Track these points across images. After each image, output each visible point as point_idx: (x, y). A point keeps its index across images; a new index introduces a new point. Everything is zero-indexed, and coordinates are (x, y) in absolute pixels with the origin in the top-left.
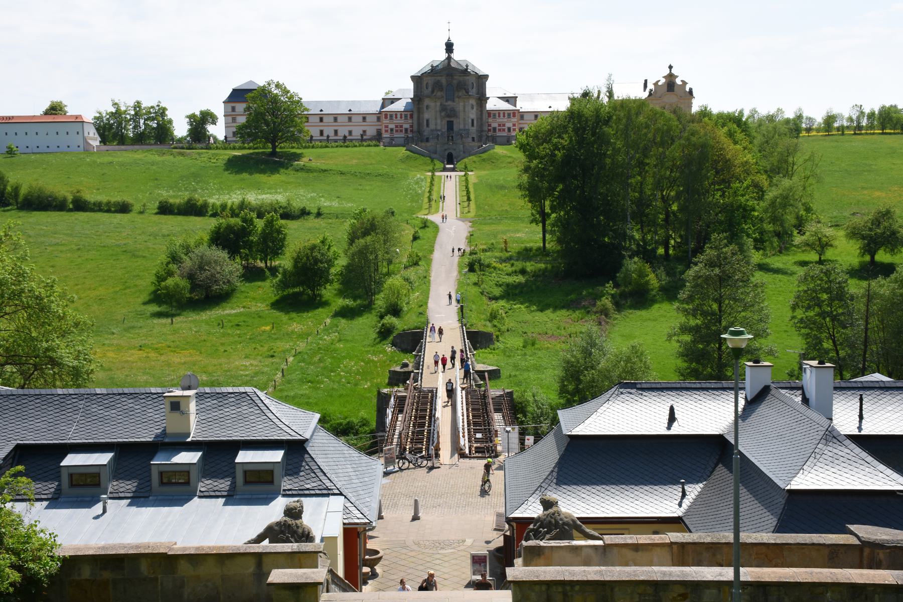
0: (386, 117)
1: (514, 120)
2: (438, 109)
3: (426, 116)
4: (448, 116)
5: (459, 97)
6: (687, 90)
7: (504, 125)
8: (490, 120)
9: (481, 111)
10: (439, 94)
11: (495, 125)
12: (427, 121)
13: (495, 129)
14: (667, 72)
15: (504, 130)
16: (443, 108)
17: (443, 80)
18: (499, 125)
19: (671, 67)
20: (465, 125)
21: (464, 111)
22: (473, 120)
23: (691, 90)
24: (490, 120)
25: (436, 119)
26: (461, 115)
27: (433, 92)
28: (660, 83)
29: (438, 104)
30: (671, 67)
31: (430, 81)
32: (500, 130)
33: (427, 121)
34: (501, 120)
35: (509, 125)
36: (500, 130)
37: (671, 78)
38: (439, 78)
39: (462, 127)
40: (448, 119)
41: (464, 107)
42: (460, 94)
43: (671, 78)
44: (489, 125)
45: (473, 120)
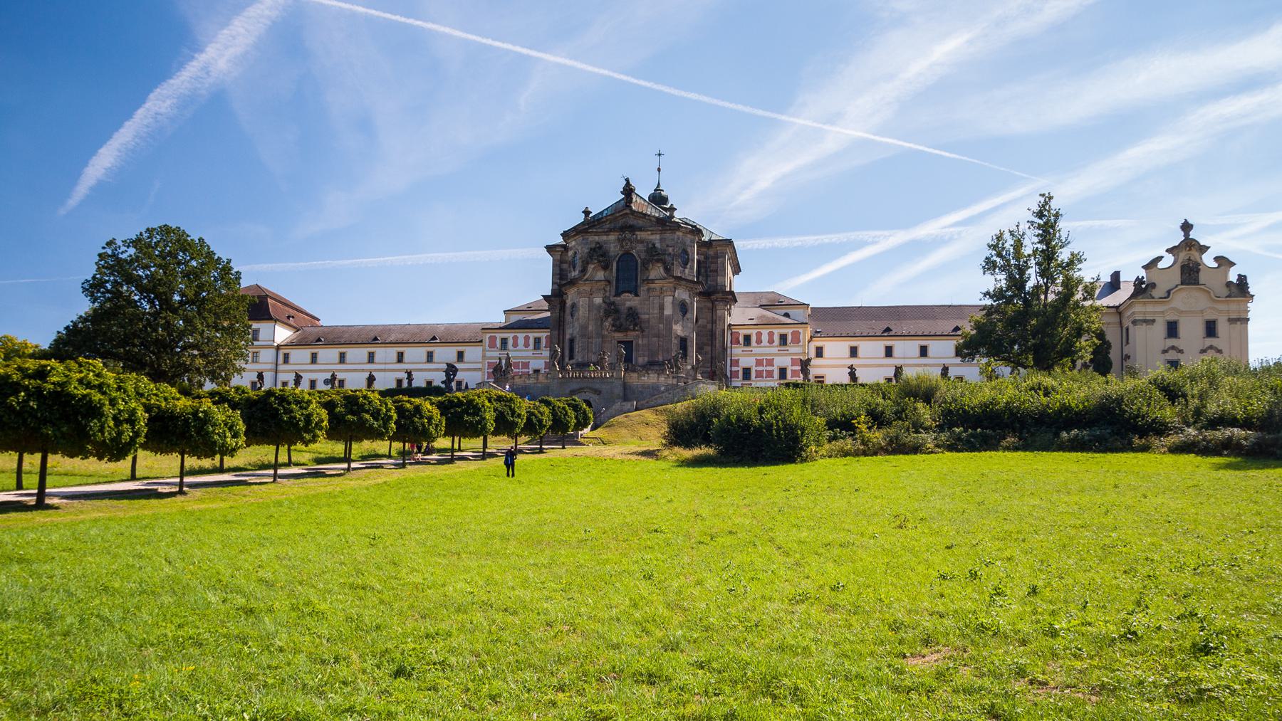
4: (618, 328)
6: (1233, 277)
7: (770, 363)
10: (600, 275)
12: (572, 341)
13: (747, 373)
14: (1179, 238)
15: (770, 374)
16: (611, 310)
18: (759, 363)
19: (1186, 227)
23: (1242, 280)
28: (1161, 265)
29: (598, 300)
30: (1186, 227)
32: (759, 374)
36: (759, 374)
37: (1189, 247)
43: (1189, 247)
44: (736, 363)
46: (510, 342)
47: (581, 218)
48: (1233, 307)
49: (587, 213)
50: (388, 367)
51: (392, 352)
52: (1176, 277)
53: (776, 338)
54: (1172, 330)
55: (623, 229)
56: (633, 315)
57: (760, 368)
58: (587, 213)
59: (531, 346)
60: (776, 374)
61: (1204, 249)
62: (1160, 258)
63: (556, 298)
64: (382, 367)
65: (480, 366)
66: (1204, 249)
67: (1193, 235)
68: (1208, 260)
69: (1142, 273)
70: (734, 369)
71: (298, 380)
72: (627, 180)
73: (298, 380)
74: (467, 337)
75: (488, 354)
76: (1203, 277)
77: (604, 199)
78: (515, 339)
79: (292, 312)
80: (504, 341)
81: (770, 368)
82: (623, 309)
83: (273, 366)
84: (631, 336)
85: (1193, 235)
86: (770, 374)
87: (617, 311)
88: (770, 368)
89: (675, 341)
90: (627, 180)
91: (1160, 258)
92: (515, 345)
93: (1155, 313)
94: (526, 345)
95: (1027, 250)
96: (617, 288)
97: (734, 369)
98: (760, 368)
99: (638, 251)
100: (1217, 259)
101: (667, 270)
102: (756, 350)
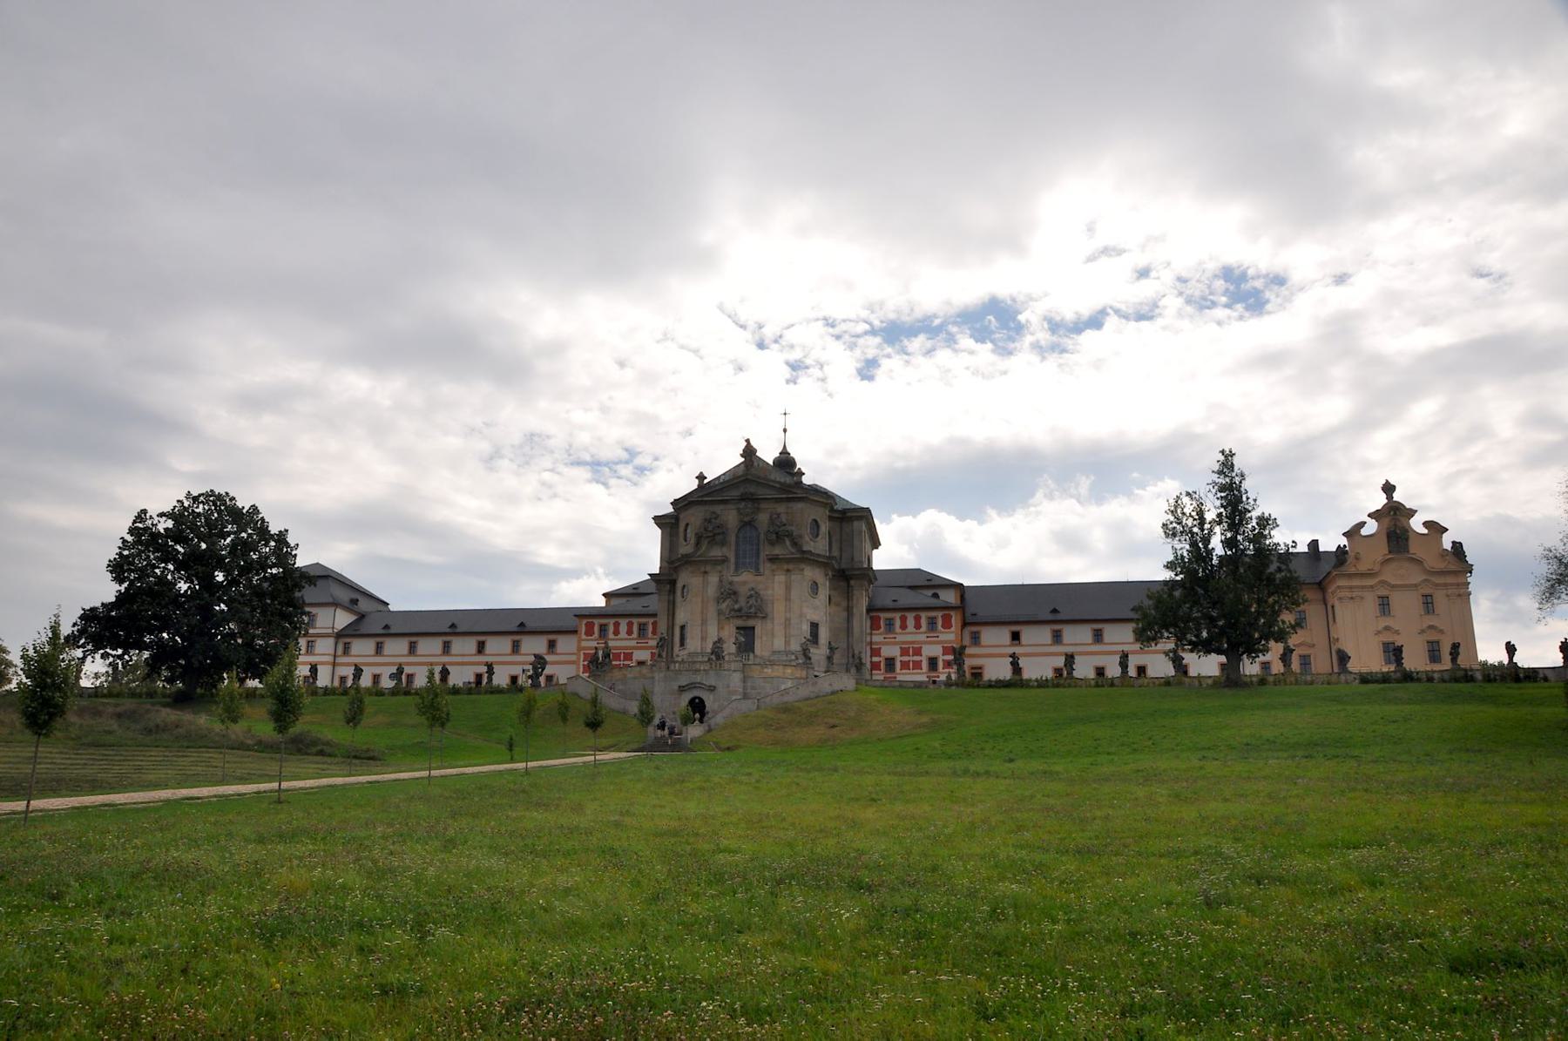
0: (589, 632)
1: (950, 636)
2: (712, 591)
3: (681, 617)
4: (738, 613)
5: (773, 559)
6: (1447, 545)
7: (918, 652)
8: (876, 639)
9: (849, 610)
10: (716, 552)
11: (888, 651)
12: (683, 628)
13: (890, 663)
14: (1380, 501)
15: (918, 665)
16: (728, 593)
17: (730, 517)
18: (904, 652)
19: (1388, 489)
20: (787, 643)
21: (788, 599)
22: (814, 626)
23: (1457, 546)
24: (876, 639)
25: (704, 622)
26: (778, 610)
27: (698, 544)
28: (1364, 532)
29: (713, 579)
30: (1388, 489)
31: (695, 518)
32: (905, 665)
33: (683, 628)
34: (911, 636)
35: (934, 650)
38: (718, 509)
39: (779, 643)
40: (740, 623)
41: (788, 588)
42: (778, 551)
45: (814, 626)
46: (611, 628)
47: (694, 485)
48: (1450, 580)
49: (701, 477)
50: (466, 659)
51: (470, 645)
52: (1383, 548)
53: (924, 622)
54: (1384, 605)
55: (743, 498)
56: (755, 595)
57: (906, 659)
58: (701, 477)
59: (635, 635)
60: (925, 665)
61: (1412, 513)
62: (1362, 524)
63: (666, 581)
64: (459, 659)
65: (574, 658)
66: (1412, 513)
67: (1397, 497)
68: (1416, 523)
69: (1344, 541)
70: (875, 659)
71: (358, 672)
72: (748, 441)
73: (358, 672)
74: (558, 625)
75: (584, 644)
76: (1415, 548)
77: (723, 461)
78: (617, 625)
79: (355, 596)
80: (603, 628)
81: (917, 658)
82: (743, 590)
83: (330, 659)
84: (750, 623)
85: (1397, 497)
86: (918, 665)
87: (735, 593)
88: (917, 658)
89: (806, 628)
90: (748, 441)
91: (1362, 524)
92: (616, 632)
93: (1363, 587)
94: (630, 632)
95: (1210, 516)
96: (737, 564)
97: (875, 659)
98: (906, 659)
99: (763, 518)
100: (1426, 524)
101: (795, 544)
102: (900, 638)
